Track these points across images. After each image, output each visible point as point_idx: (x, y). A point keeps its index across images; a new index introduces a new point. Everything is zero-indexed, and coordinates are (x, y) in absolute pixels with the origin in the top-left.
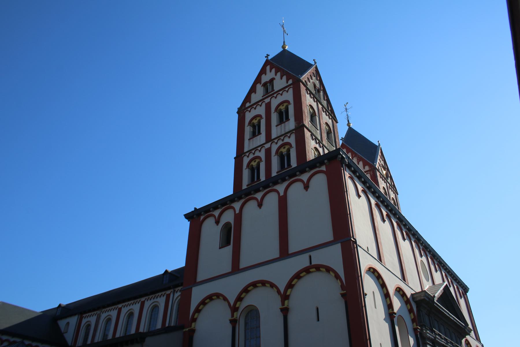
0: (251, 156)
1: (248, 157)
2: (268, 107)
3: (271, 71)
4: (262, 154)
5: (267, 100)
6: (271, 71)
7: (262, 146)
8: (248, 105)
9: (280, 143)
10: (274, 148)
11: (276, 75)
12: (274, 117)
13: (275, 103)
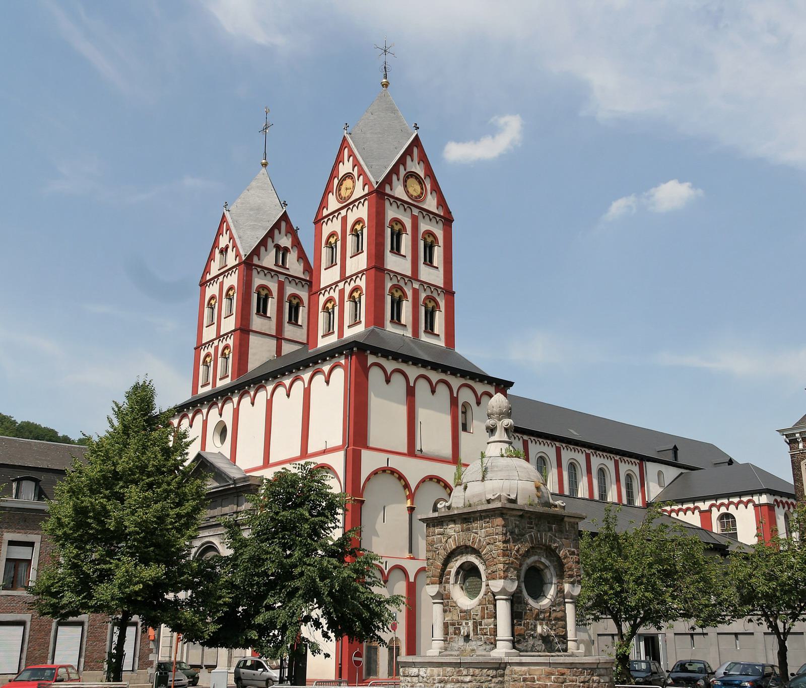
0: (327, 295)
1: (324, 295)
2: (344, 219)
3: (348, 161)
4: (336, 295)
5: (343, 212)
6: (348, 161)
7: (336, 284)
8: (325, 212)
9: (353, 284)
10: (348, 289)
11: (353, 171)
12: (350, 239)
13: (351, 219)
